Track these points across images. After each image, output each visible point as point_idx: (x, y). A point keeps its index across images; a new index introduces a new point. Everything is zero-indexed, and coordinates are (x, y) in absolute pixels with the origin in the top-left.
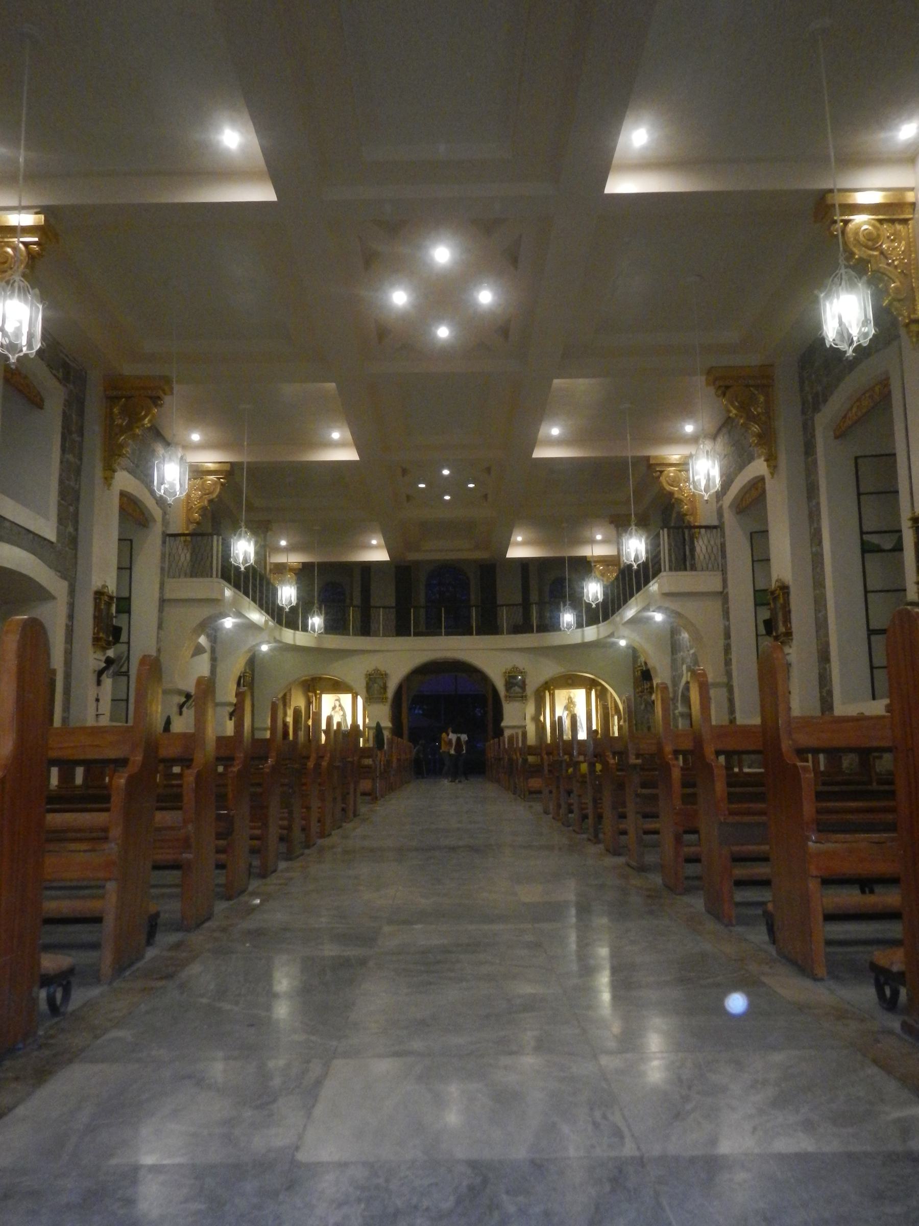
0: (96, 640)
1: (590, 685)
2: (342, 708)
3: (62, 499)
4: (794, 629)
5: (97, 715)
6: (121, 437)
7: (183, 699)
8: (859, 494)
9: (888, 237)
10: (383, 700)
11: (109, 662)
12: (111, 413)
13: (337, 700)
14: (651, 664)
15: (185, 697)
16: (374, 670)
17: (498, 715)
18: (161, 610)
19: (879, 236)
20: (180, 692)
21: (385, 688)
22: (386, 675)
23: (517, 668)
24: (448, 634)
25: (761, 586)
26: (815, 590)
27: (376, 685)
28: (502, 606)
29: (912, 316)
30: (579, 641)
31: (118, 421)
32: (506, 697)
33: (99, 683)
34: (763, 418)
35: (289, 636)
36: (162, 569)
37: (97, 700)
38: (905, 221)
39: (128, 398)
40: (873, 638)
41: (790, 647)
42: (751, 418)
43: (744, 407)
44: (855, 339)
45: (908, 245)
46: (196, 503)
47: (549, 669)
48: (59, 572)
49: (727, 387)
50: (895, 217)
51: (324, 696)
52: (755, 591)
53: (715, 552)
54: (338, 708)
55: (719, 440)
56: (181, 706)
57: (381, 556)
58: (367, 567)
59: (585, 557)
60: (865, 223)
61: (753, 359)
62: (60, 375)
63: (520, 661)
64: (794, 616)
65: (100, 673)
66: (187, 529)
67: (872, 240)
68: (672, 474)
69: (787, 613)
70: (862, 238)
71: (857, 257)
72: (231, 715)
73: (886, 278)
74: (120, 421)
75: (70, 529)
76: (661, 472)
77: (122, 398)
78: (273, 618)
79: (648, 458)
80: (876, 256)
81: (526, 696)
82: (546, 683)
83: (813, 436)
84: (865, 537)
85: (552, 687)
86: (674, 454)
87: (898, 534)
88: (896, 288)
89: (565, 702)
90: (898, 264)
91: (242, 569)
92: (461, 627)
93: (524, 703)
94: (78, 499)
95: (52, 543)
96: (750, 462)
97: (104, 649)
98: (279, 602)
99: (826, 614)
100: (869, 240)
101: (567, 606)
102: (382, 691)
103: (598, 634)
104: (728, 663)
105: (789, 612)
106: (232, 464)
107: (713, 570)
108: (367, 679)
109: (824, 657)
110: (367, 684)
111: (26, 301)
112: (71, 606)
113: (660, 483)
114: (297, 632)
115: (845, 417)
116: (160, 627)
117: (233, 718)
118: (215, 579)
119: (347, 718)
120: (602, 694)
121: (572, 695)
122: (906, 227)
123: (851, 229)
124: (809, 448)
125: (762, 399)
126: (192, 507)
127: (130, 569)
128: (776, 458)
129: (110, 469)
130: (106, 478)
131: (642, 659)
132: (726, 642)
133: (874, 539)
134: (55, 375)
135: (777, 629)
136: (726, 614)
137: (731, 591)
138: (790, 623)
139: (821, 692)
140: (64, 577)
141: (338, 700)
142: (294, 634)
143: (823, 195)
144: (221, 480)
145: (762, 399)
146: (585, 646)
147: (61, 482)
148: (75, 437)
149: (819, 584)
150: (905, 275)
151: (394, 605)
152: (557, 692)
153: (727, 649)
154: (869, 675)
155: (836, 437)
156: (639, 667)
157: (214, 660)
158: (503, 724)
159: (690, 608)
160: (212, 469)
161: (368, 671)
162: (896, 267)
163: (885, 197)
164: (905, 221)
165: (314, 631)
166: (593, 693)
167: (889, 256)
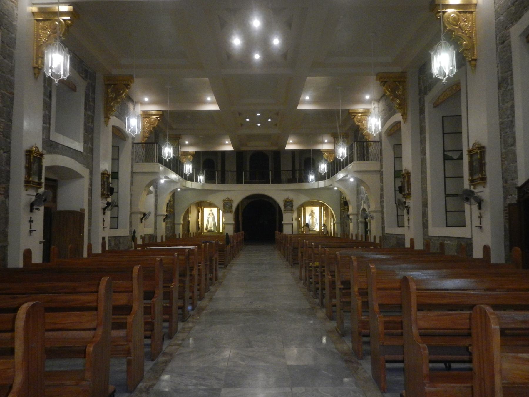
0: (102, 194)
1: (321, 205)
3: (86, 132)
4: (412, 192)
5: (104, 228)
6: (112, 102)
7: (142, 216)
8: (444, 134)
9: (463, 20)
10: (231, 212)
11: (108, 204)
12: (108, 91)
13: (211, 211)
14: (348, 198)
15: (144, 215)
16: (227, 199)
17: (281, 219)
18: (132, 177)
19: (459, 19)
20: (141, 213)
21: (231, 207)
22: (232, 201)
23: (289, 198)
24: (259, 183)
25: (397, 169)
26: (422, 175)
27: (227, 205)
28: (283, 171)
29: (473, 58)
30: (316, 187)
32: (284, 211)
33: (104, 213)
35: (189, 184)
36: (132, 159)
37: (104, 221)
38: (471, 12)
39: (115, 85)
40: (448, 198)
41: (410, 200)
42: (396, 96)
43: (393, 91)
44: (447, 74)
45: (472, 24)
46: (147, 128)
47: (304, 199)
48: (85, 165)
49: (386, 82)
50: (467, 10)
51: (205, 209)
52: (395, 171)
53: (377, 153)
54: (211, 214)
55: (381, 102)
56: (142, 219)
57: (230, 148)
58: (224, 153)
59: (320, 150)
60: (453, 13)
61: (397, 69)
62: (83, 76)
63: (291, 195)
65: (105, 209)
66: (143, 140)
67: (456, 20)
68: (359, 117)
69: (409, 184)
70: (451, 21)
71: (448, 29)
72: (164, 220)
73: (461, 39)
74: (111, 95)
75: (90, 145)
76: (355, 116)
77: (112, 84)
78: (182, 177)
79: (349, 110)
80: (456, 29)
81: (293, 211)
82: (302, 204)
83: (424, 106)
84: (446, 153)
85: (304, 206)
86: (360, 108)
87: (461, 152)
88: (466, 45)
89: (310, 212)
90: (467, 33)
91: (167, 160)
92: (264, 180)
93: (292, 213)
94: (93, 131)
95: (81, 152)
96: (394, 114)
97: (106, 198)
98: (184, 171)
99: (427, 186)
100: (454, 21)
102: (230, 208)
105: (410, 184)
106: (163, 111)
108: (224, 203)
109: (425, 205)
110: (224, 205)
111: (62, 55)
112: (91, 180)
113: (354, 121)
114: (193, 182)
115: (439, 98)
116: (132, 184)
117: (165, 221)
118: (157, 163)
120: (326, 209)
121: (313, 210)
122: (471, 15)
123: (446, 16)
124: (422, 111)
125: (401, 87)
126: (145, 130)
127: (118, 159)
128: (406, 114)
129: (107, 117)
130: (105, 121)
132: (381, 193)
134: (81, 76)
135: (404, 191)
136: (382, 180)
138: (410, 189)
139: (423, 220)
140: (87, 167)
141: (211, 211)
142: (192, 183)
144: (158, 118)
145: (401, 87)
146: (319, 189)
147: (85, 125)
148: (91, 104)
149: (424, 172)
150: (470, 38)
151: (235, 169)
152: (306, 208)
153: (382, 196)
156: (343, 199)
157: (156, 196)
158: (283, 222)
159: (365, 177)
160: (154, 113)
161: (224, 199)
162: (466, 34)
164: (471, 12)
165: (200, 182)
166: (322, 208)
167: (463, 29)
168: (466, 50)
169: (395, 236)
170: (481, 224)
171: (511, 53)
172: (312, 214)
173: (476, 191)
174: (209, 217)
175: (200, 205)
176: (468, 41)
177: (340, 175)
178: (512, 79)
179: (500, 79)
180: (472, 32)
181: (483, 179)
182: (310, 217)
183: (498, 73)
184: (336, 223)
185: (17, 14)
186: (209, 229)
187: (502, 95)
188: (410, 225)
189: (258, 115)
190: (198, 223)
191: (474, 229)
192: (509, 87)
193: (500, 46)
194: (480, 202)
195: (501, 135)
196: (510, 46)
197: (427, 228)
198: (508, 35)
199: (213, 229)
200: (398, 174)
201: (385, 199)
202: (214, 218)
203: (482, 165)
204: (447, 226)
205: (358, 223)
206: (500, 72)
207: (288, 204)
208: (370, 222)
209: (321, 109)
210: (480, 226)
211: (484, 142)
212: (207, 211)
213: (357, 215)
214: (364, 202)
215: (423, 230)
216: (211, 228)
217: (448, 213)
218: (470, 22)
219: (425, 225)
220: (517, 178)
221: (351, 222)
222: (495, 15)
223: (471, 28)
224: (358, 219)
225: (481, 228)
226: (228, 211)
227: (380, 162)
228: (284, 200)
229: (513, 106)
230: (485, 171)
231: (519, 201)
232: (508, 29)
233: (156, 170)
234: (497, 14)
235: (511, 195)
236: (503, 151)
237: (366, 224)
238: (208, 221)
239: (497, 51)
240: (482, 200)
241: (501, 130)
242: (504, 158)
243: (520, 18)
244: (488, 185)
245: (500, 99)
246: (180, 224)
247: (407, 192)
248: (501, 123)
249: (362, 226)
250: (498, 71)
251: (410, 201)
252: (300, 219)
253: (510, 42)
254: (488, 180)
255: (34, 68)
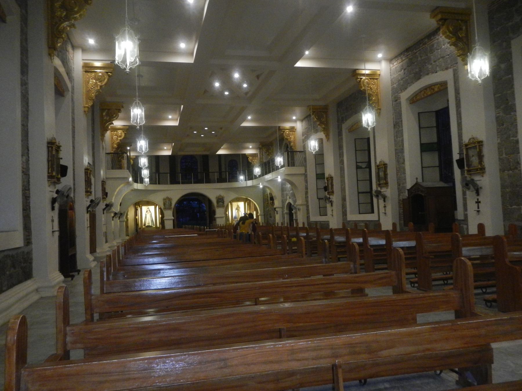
1: (245, 200)
2: (150, 212)
4: (335, 191)
8: (356, 150)
10: (170, 208)
17: (212, 213)
30: (245, 185)
31: (105, 118)
32: (217, 206)
34: (325, 122)
39: (109, 110)
40: (360, 194)
51: (143, 207)
52: (317, 174)
54: (148, 212)
55: (304, 122)
61: (321, 103)
63: (222, 193)
64: (334, 187)
65: (104, 210)
66: (112, 150)
70: (365, 84)
76: (284, 132)
77: (106, 109)
79: (279, 127)
83: (341, 130)
84: (358, 164)
86: (287, 125)
88: (375, 100)
92: (198, 181)
101: (242, 174)
103: (253, 184)
104: (307, 197)
105: (333, 185)
107: (302, 166)
109: (344, 199)
118: (126, 170)
119: (152, 215)
121: (239, 204)
124: (340, 134)
128: (329, 136)
131: (268, 191)
133: (360, 164)
137: (308, 173)
139: (342, 210)
143: (355, 70)
145: (325, 116)
149: (342, 176)
153: (307, 193)
154: (358, 205)
155: (349, 132)
158: (217, 216)
162: (374, 93)
163: (372, 72)
164: (377, 79)
165: (145, 183)
168: (375, 103)
169: (319, 222)
170: (385, 211)
171: (401, 108)
172: (238, 209)
173: (382, 190)
174: (146, 213)
175: (138, 204)
176: (375, 97)
177: (268, 177)
178: (402, 124)
179: (394, 122)
180: (378, 92)
181: (386, 184)
182: (237, 211)
183: (393, 119)
184: (261, 215)
185: (74, 68)
186: (147, 225)
187: (396, 132)
188: (333, 214)
189: (206, 129)
190: (136, 220)
191: (381, 215)
192: (400, 129)
193: (394, 103)
194: (384, 198)
195: (396, 157)
196: (400, 103)
197: (346, 215)
198: (399, 97)
199: (150, 224)
200: (320, 176)
201: (309, 195)
202: (151, 214)
203: (386, 175)
204: (360, 213)
205: (283, 214)
206: (394, 118)
207: (220, 200)
208: (296, 213)
209: (260, 126)
210: (385, 212)
211: (387, 161)
212: (144, 208)
213: (283, 208)
214: (290, 198)
215: (343, 217)
216: (148, 223)
217: (360, 204)
218: (377, 85)
219: (344, 214)
220: (406, 183)
221: (277, 214)
222: (391, 82)
223: (377, 89)
224: (283, 212)
225: (385, 213)
226: (167, 208)
227: (304, 167)
228: (217, 197)
229: (403, 140)
230: (387, 179)
231: (409, 197)
232: (399, 93)
233: (125, 176)
234: (392, 83)
235: (403, 193)
236: (397, 166)
237: (291, 215)
238: (146, 217)
239: (393, 105)
240: (386, 197)
241: (396, 153)
242: (398, 171)
243: (406, 89)
244: (389, 187)
245: (395, 135)
246: (124, 221)
247: (331, 191)
248: (396, 150)
249: (287, 217)
250: (393, 118)
251: (333, 197)
252: (227, 213)
253: (400, 101)
254: (389, 184)
255: (85, 107)
